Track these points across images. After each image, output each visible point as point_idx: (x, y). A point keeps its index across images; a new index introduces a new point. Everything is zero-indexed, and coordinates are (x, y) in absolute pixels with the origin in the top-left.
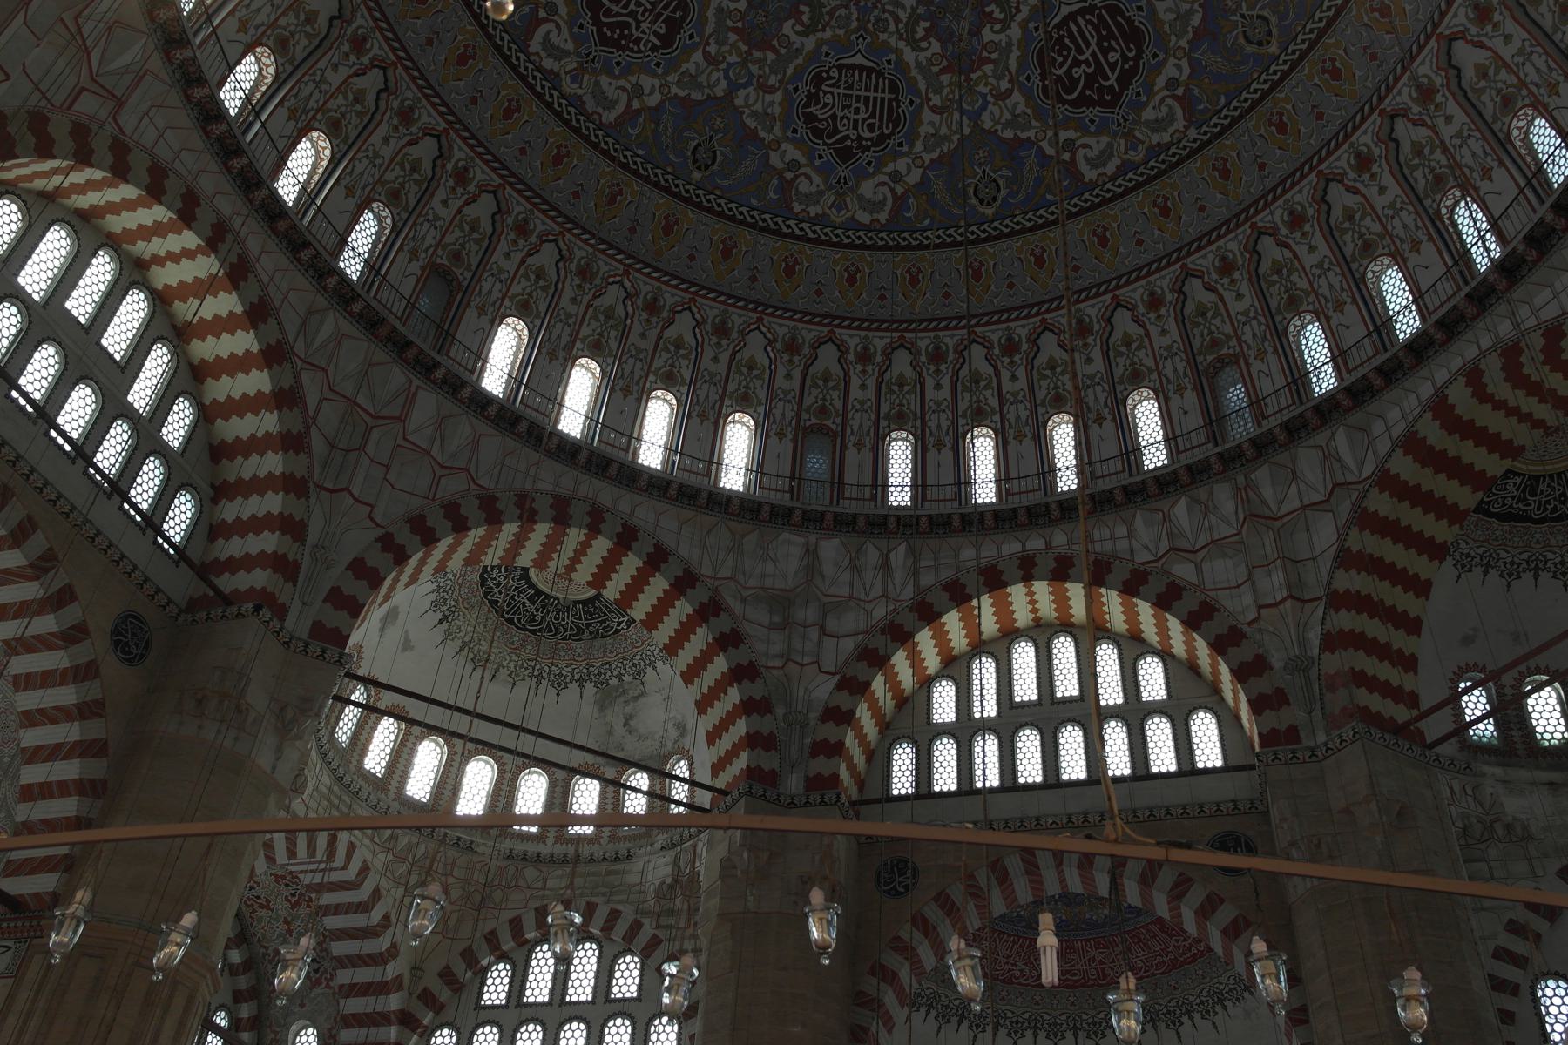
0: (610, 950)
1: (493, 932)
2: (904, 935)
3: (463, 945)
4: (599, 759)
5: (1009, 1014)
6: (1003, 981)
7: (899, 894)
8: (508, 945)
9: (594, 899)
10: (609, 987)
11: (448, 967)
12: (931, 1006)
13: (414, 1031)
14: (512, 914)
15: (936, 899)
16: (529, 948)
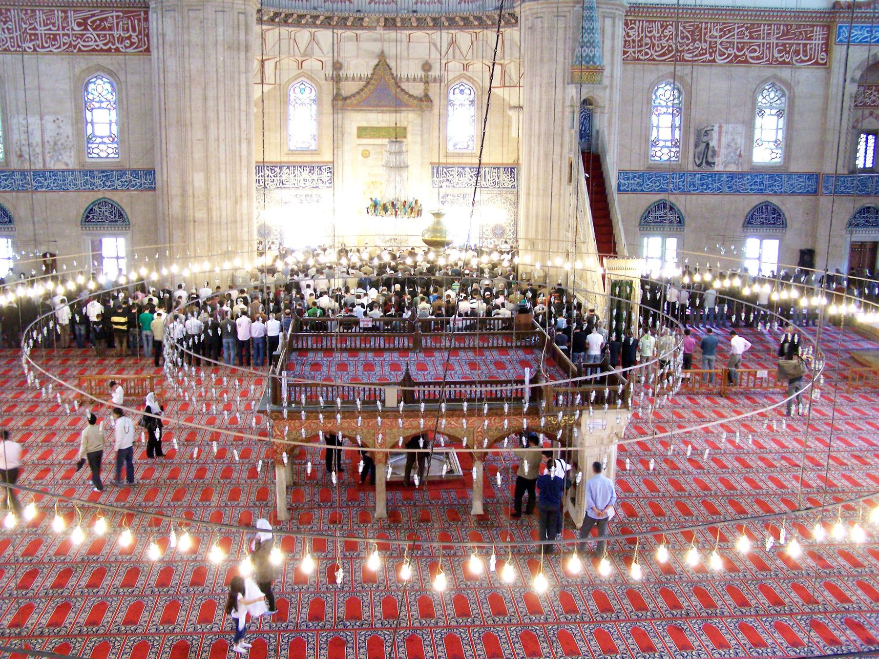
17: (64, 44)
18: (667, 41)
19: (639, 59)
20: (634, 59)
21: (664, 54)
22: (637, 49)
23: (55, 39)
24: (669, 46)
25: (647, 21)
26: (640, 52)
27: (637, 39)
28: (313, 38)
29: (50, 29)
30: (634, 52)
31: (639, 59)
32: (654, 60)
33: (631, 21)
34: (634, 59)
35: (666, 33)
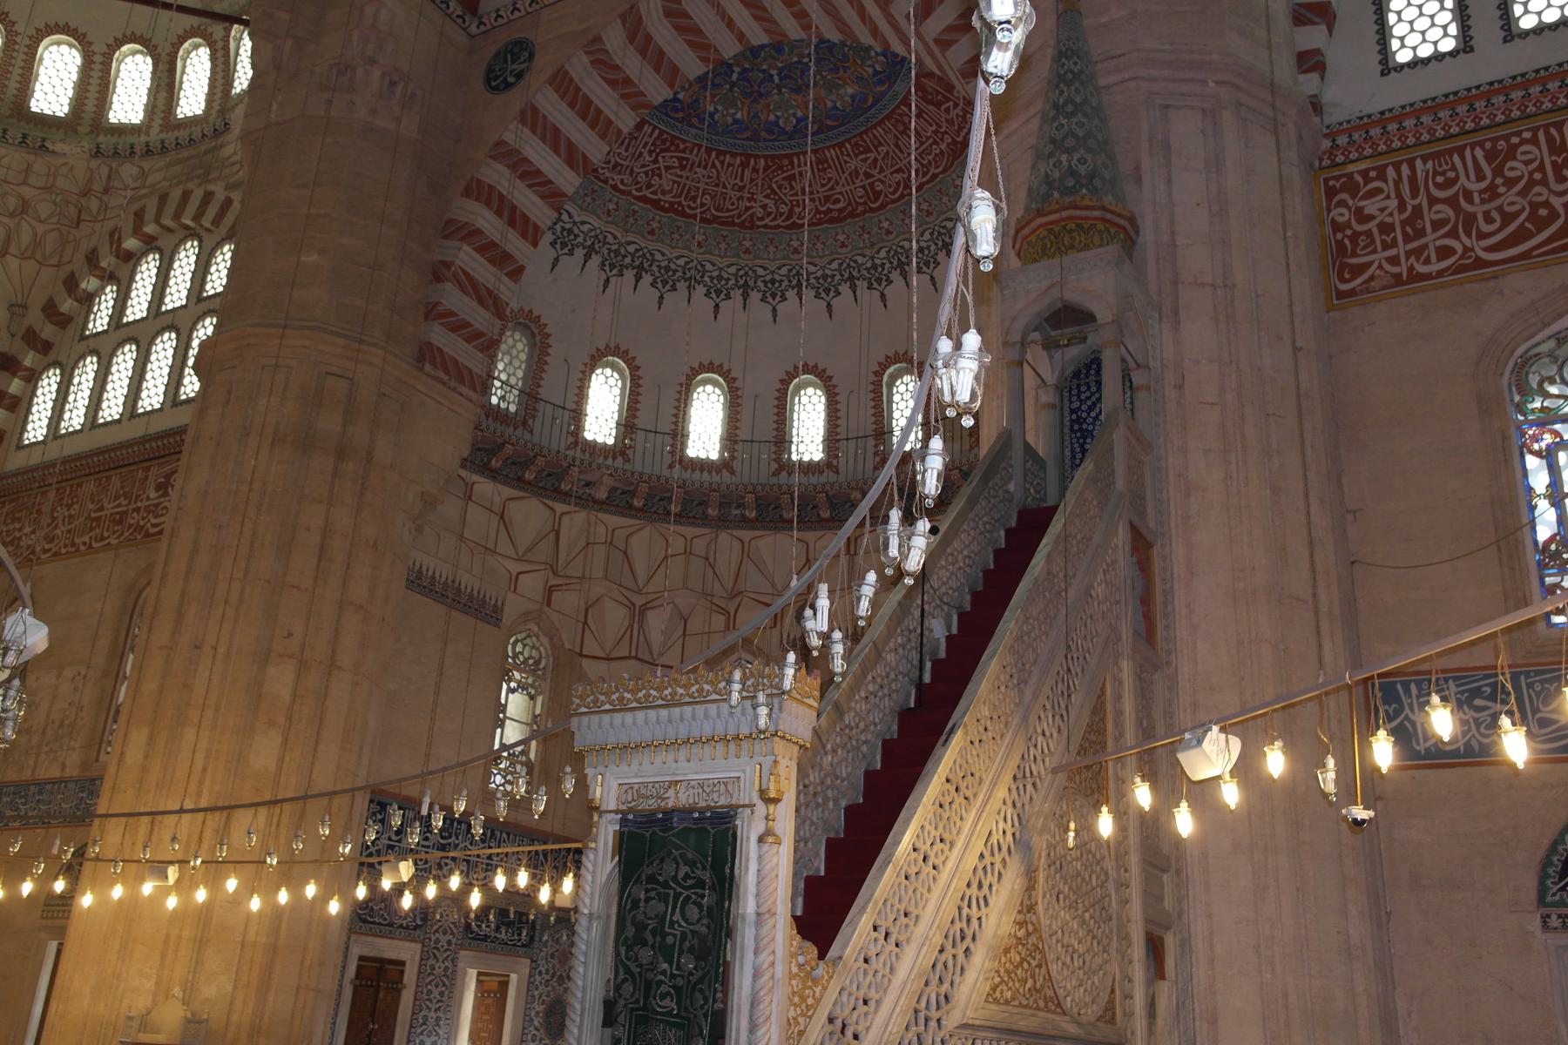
0: (210, 241)
1: (94, 250)
2: (509, 137)
3: (65, 272)
4: (205, 20)
5: (761, 272)
6: (742, 225)
7: (509, 86)
8: (107, 261)
9: (190, 185)
10: (203, 282)
11: (51, 299)
12: (641, 268)
13: (14, 375)
14: (109, 225)
15: (551, 82)
16: (131, 260)
17: (130, 526)
18: (1523, 193)
19: (1414, 277)
20: (1398, 280)
21: (1521, 236)
22: (1401, 249)
23: (120, 522)
24: (1534, 206)
25: (1425, 159)
26: (1417, 253)
27: (1397, 219)
28: (745, 553)
29: (120, 505)
30: (1394, 261)
31: (1414, 277)
32: (1480, 263)
33: (1364, 173)
34: (1398, 280)
35: (1515, 168)
